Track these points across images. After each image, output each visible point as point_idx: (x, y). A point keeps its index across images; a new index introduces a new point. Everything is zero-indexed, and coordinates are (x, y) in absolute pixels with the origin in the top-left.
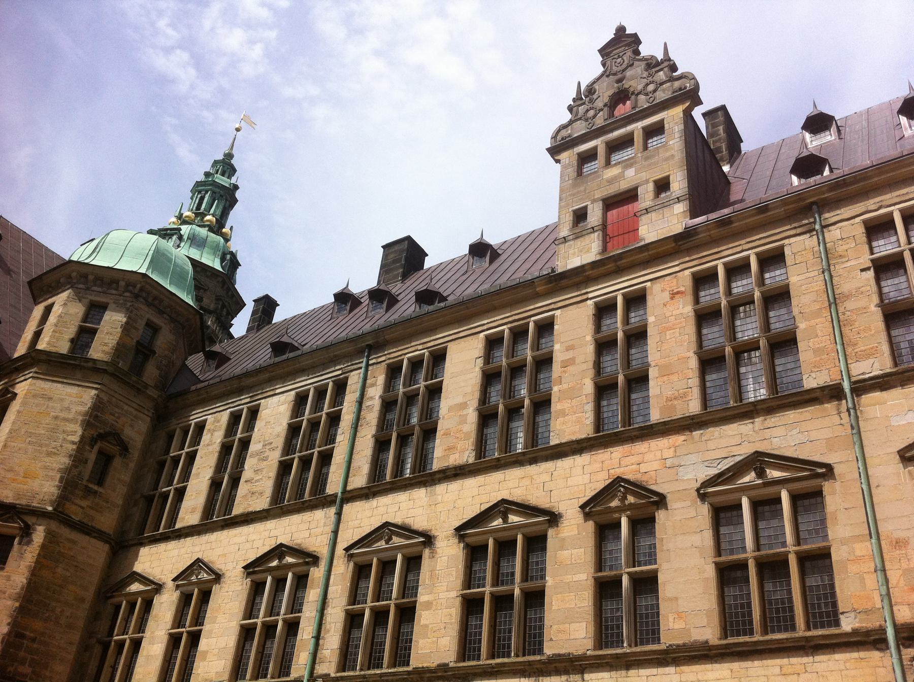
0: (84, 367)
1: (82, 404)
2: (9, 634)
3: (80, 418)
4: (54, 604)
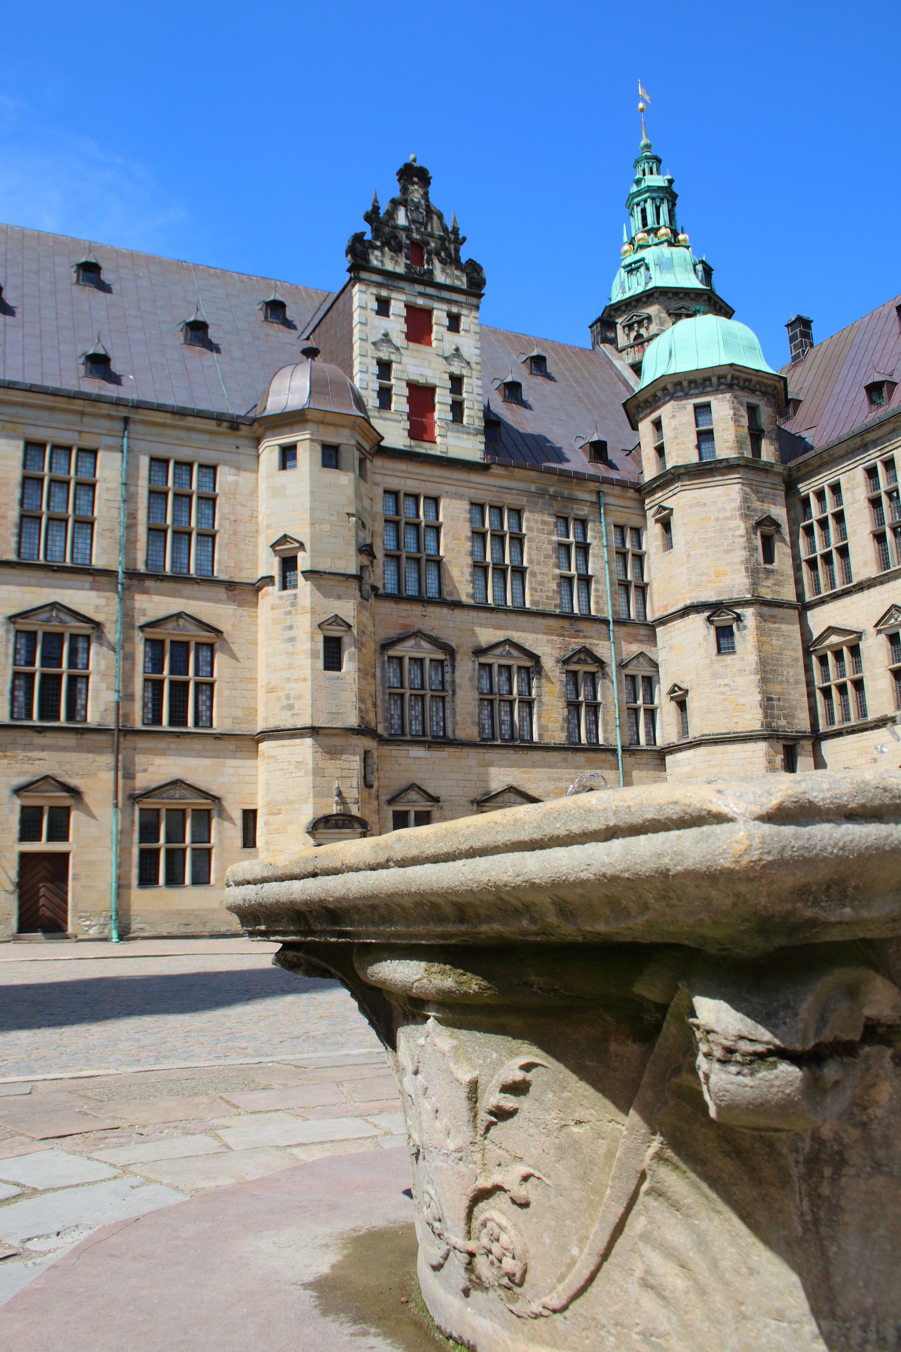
1: (733, 500)
2: (762, 700)
3: (737, 513)
4: (780, 669)
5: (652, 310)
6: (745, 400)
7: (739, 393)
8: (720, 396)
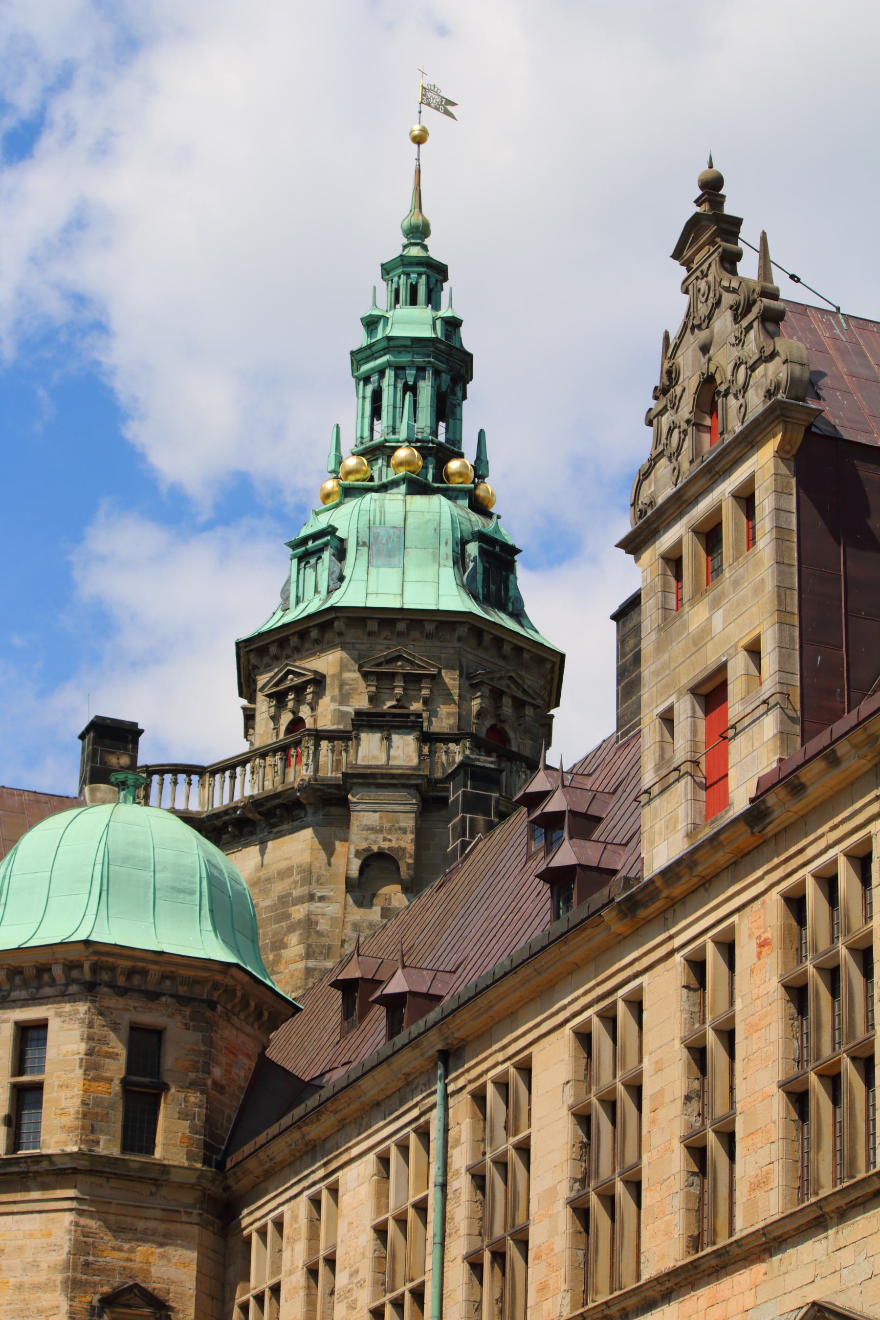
0: (37, 1174)
3: (59, 1277)
5: (328, 662)
6: (127, 1018)
7: (113, 1002)
8: (68, 1007)
